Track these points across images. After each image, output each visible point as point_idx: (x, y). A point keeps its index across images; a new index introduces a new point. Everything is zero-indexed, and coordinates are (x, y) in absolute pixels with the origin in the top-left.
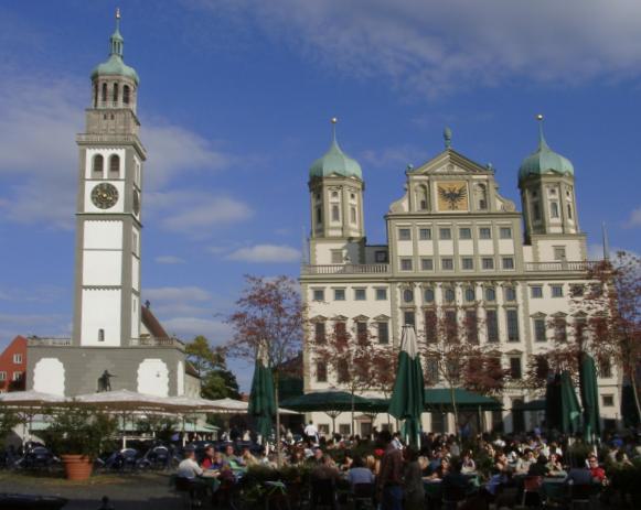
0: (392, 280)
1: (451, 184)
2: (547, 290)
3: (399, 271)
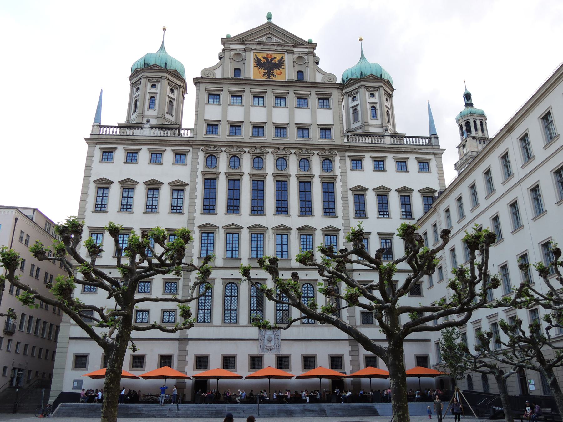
2: (368, 163)
3: (202, 135)
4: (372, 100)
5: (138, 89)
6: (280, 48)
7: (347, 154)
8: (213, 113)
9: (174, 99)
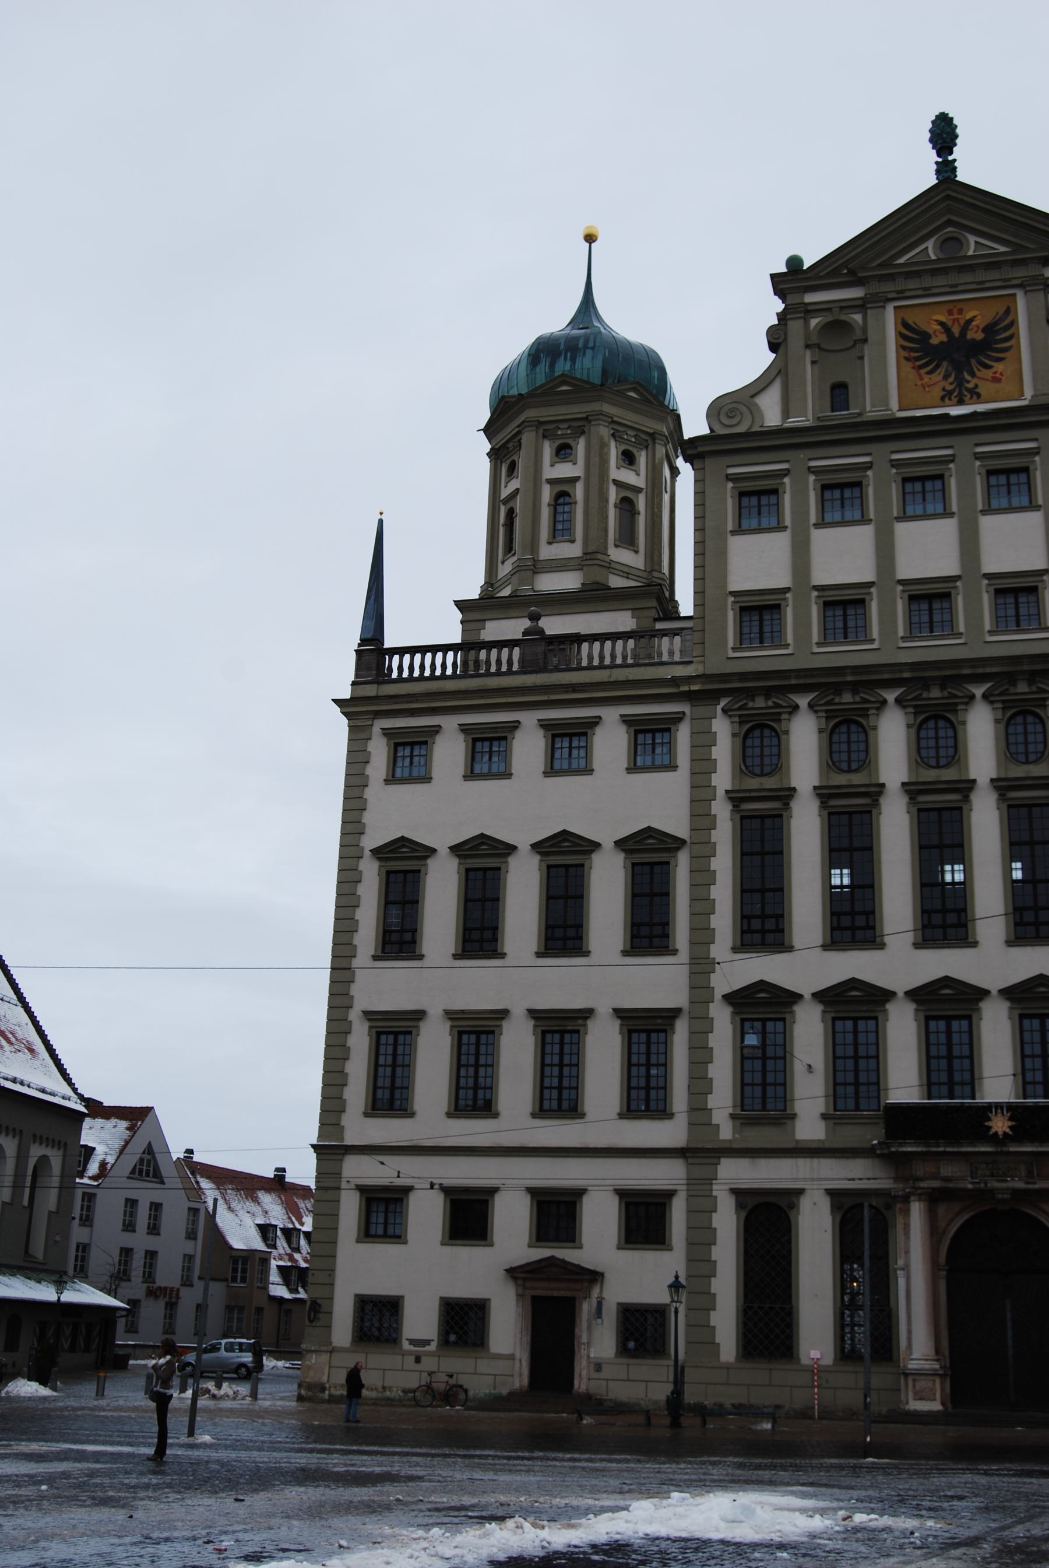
0: (705, 693)
1: (952, 308)
3: (729, 652)
5: (512, 468)
6: (994, 275)
8: (759, 562)
9: (638, 490)
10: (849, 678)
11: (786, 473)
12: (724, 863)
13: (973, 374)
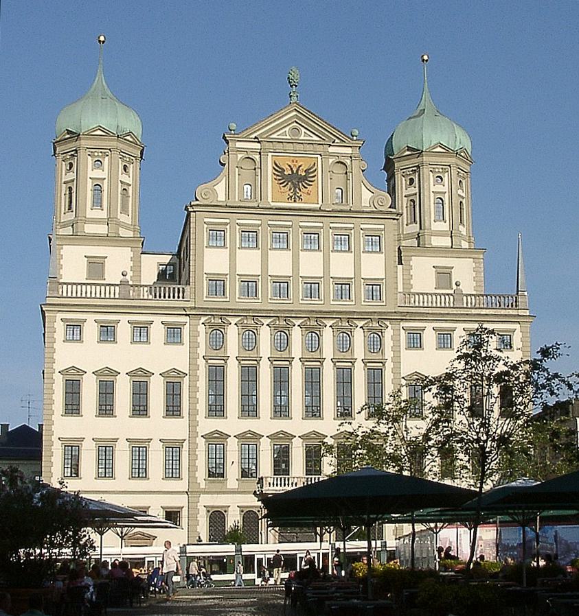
0: (194, 313)
4: (439, 188)
5: (71, 165)
7: (403, 324)
10: (251, 314)
11: (226, 224)
12: (202, 383)
13: (300, 190)
